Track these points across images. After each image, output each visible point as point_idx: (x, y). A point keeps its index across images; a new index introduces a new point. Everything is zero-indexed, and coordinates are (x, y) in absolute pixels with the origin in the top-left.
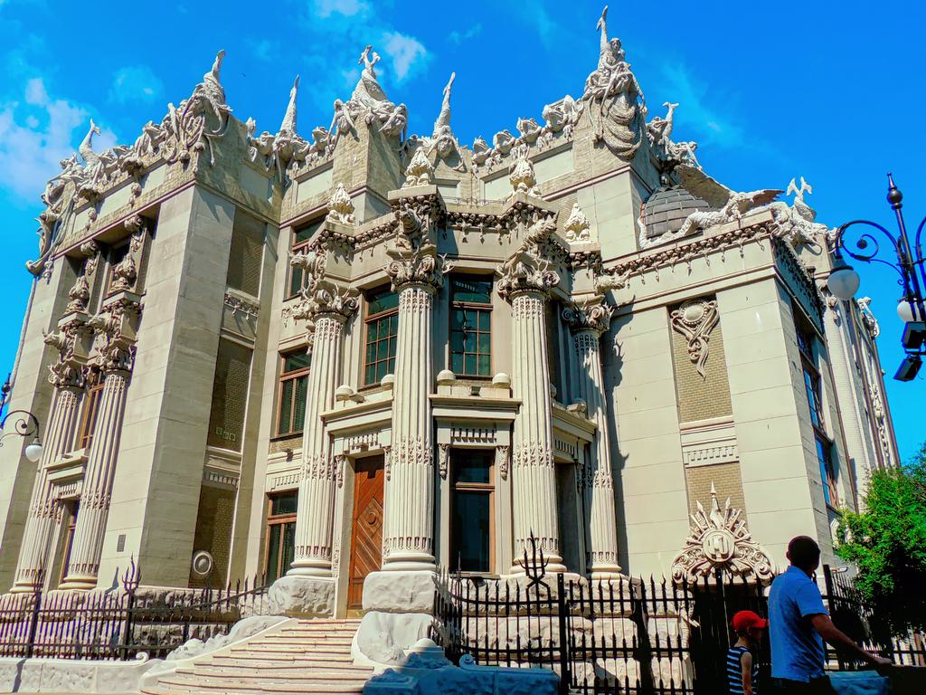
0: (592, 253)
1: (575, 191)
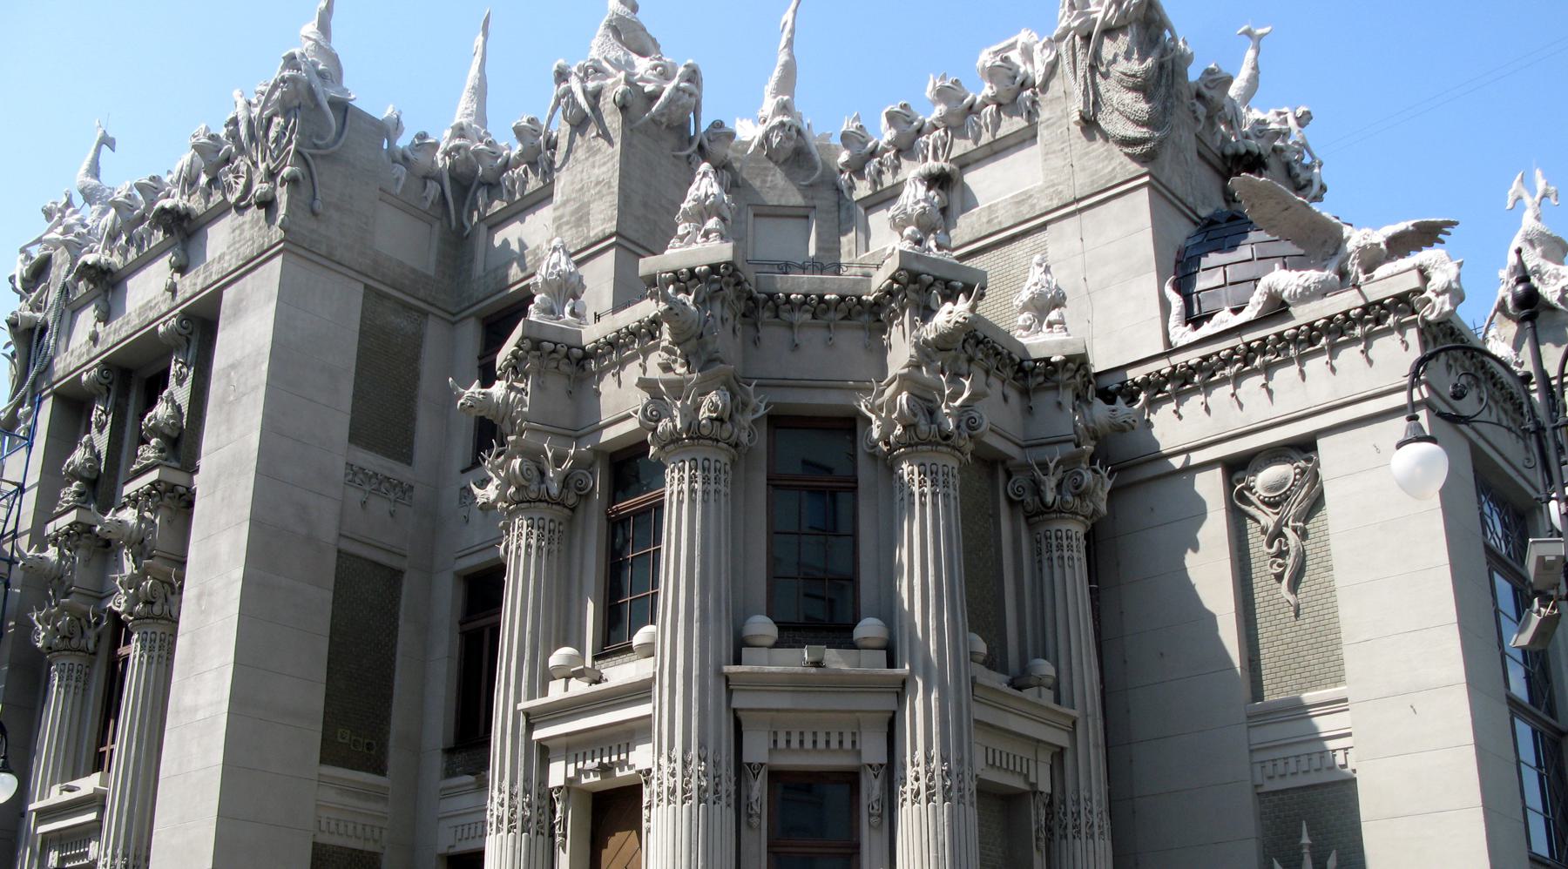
0: (1069, 359)
1: (1043, 227)
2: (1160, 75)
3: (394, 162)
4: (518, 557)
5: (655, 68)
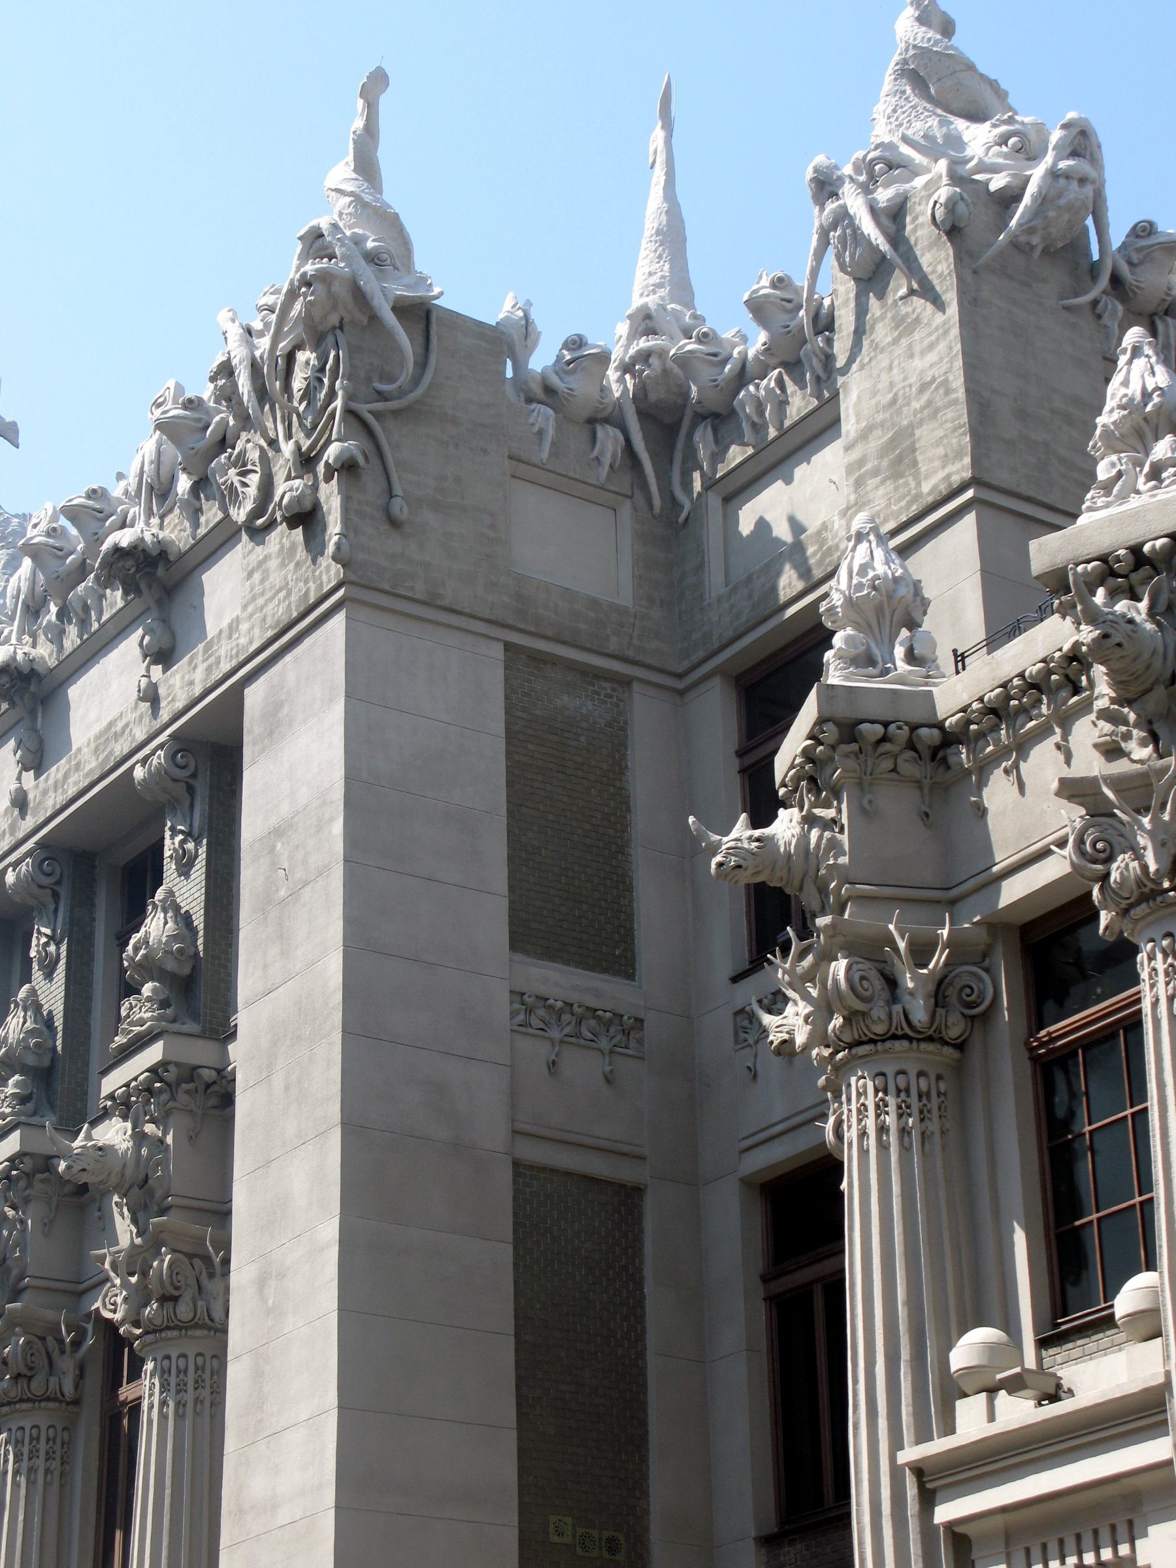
3: (529, 400)
4: (864, 1153)
5: (1003, 140)
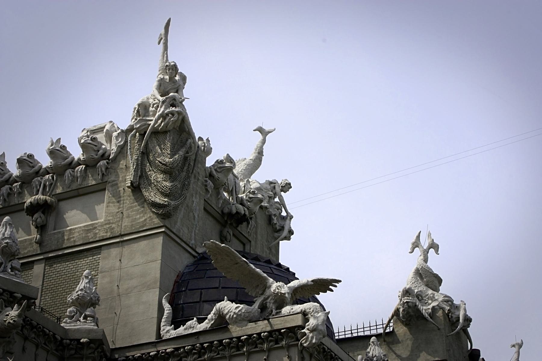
0: (91, 341)
2: (184, 164)
